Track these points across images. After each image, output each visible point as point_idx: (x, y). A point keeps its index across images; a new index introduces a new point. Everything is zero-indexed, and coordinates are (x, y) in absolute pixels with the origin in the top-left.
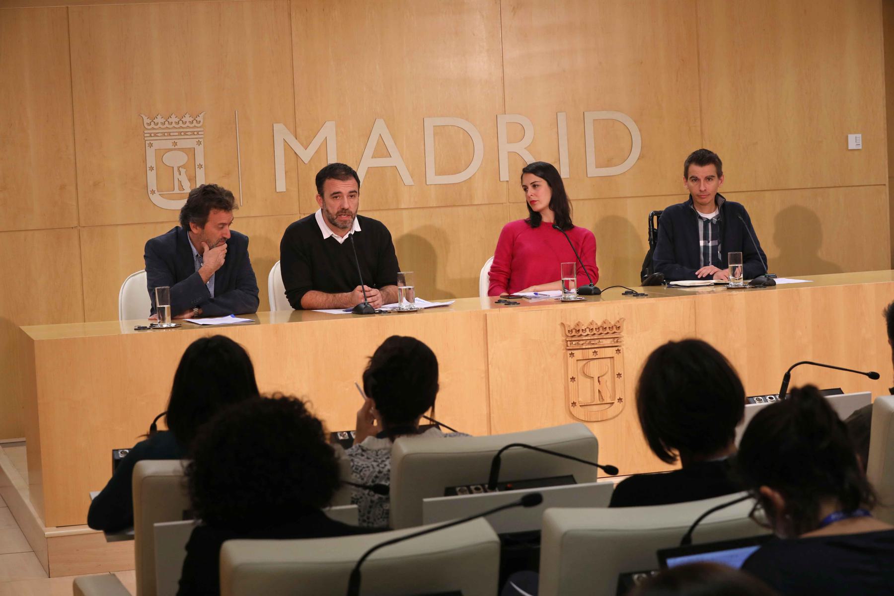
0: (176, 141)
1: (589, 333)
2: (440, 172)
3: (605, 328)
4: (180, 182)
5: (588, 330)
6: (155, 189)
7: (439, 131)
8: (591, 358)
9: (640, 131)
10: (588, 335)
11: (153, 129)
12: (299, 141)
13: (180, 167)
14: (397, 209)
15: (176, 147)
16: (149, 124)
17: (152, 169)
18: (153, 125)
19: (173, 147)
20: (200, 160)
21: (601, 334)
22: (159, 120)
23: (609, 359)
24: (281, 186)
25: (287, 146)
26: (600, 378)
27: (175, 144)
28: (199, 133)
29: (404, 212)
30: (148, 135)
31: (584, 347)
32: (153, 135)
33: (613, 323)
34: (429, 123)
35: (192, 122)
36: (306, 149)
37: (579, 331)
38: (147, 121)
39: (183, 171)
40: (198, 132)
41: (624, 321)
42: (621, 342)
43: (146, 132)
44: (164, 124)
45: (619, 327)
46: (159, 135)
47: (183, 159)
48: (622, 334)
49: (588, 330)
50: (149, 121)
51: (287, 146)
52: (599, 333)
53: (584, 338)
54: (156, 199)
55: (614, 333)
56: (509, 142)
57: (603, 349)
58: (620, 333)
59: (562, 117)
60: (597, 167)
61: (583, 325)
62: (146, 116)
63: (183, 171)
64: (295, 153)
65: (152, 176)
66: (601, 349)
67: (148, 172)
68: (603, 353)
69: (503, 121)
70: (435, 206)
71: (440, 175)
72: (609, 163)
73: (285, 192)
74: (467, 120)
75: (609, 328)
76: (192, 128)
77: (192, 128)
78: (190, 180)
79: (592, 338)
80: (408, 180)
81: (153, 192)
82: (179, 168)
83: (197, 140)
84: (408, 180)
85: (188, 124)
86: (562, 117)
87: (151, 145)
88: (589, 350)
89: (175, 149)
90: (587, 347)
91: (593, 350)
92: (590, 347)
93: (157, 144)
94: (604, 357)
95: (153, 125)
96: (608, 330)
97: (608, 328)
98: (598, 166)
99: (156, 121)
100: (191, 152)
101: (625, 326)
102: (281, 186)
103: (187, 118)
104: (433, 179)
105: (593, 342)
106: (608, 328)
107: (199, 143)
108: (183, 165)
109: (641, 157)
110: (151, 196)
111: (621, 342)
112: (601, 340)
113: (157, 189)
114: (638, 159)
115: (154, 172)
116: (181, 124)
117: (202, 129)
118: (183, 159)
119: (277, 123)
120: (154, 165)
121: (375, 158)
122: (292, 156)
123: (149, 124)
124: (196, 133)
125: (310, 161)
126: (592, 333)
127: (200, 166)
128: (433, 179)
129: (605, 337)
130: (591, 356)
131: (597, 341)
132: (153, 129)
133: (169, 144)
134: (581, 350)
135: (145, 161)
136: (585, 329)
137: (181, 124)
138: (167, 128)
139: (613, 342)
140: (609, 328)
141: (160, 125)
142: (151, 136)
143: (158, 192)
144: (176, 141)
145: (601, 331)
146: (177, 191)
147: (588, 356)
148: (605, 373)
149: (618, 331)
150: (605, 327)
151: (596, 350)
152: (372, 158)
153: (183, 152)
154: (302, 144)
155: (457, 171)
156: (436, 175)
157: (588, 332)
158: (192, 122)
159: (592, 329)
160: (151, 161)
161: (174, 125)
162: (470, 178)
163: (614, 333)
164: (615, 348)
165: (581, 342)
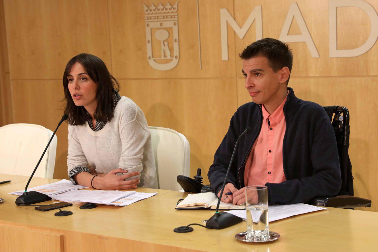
0: (162, 22)
4: (164, 51)
6: (151, 56)
11: (149, 14)
12: (237, 23)
13: (165, 41)
14: (307, 77)
15: (163, 27)
16: (147, 11)
17: (149, 42)
18: (149, 11)
19: (160, 27)
20: (176, 36)
22: (153, 8)
27: (161, 24)
28: (176, 17)
29: (312, 80)
30: (146, 18)
32: (149, 18)
35: (170, 9)
36: (241, 28)
38: (146, 8)
39: (166, 43)
40: (174, 16)
43: (146, 16)
44: (154, 10)
46: (153, 18)
47: (165, 35)
50: (147, 8)
54: (151, 62)
62: (145, 5)
63: (166, 43)
64: (235, 32)
65: (149, 46)
67: (148, 44)
70: (336, 75)
71: (342, 48)
73: (227, 61)
76: (172, 12)
77: (172, 12)
78: (170, 50)
80: (314, 53)
81: (150, 58)
82: (164, 41)
83: (174, 22)
84: (314, 53)
85: (168, 10)
87: (148, 25)
89: (163, 28)
93: (152, 25)
95: (149, 11)
99: (151, 8)
100: (169, 30)
102: (225, 57)
103: (168, 6)
107: (175, 24)
108: (167, 39)
110: (149, 60)
113: (152, 55)
115: (150, 44)
116: (165, 11)
117: (176, 14)
118: (165, 35)
119: (222, 7)
120: (150, 40)
121: (290, 35)
122: (231, 33)
123: (147, 11)
124: (173, 17)
127: (175, 41)
128: (334, 53)
132: (149, 14)
133: (158, 25)
135: (145, 37)
137: (165, 11)
138: (157, 13)
141: (153, 11)
142: (148, 19)
143: (153, 57)
144: (162, 22)
146: (163, 58)
152: (288, 35)
153: (167, 30)
155: (355, 47)
156: (337, 49)
158: (170, 9)
160: (148, 37)
161: (161, 11)
162: (367, 52)
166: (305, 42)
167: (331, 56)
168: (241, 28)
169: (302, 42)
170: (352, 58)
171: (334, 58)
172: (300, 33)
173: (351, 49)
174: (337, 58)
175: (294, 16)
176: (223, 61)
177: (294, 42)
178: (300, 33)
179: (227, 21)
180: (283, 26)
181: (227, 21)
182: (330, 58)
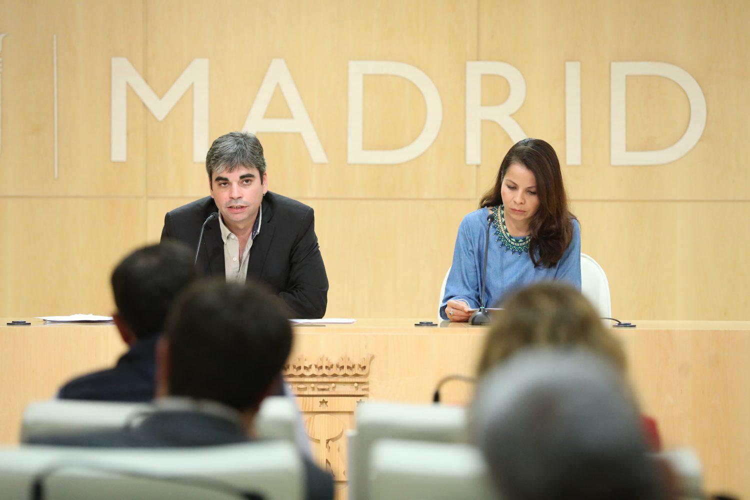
1: (316, 373)
2: (368, 146)
3: (343, 367)
5: (313, 367)
7: (372, 82)
8: (317, 410)
9: (705, 95)
10: (313, 376)
21: (335, 375)
23: (347, 416)
24: (119, 152)
25: (131, 93)
26: (330, 442)
31: (306, 393)
33: (356, 361)
34: (357, 70)
36: (160, 97)
37: (300, 368)
41: (373, 357)
42: (367, 390)
45: (364, 367)
48: (370, 378)
49: (313, 367)
51: (131, 93)
52: (332, 374)
53: (306, 380)
55: (356, 375)
56: (485, 103)
57: (337, 398)
58: (366, 376)
59: (573, 70)
60: (628, 149)
61: (306, 360)
64: (144, 106)
66: (334, 398)
68: (335, 404)
69: (475, 70)
72: (649, 145)
73: (123, 162)
74: (418, 67)
75: (348, 367)
79: (320, 380)
80: (318, 154)
84: (318, 154)
86: (573, 70)
88: (314, 398)
90: (312, 393)
91: (321, 399)
92: (315, 393)
94: (337, 410)
96: (346, 371)
97: (345, 368)
98: (628, 149)
101: (374, 368)
102: (119, 152)
104: (357, 154)
105: (321, 387)
106: (345, 368)
109: (704, 137)
111: (367, 390)
112: (333, 385)
114: (700, 140)
125: (166, 118)
126: (320, 373)
129: (341, 380)
130: (317, 408)
131: (326, 387)
134: (302, 398)
136: (310, 366)
139: (354, 389)
140: (348, 367)
145: (334, 371)
147: (313, 408)
148: (337, 435)
149: (361, 374)
150: (341, 365)
151: (326, 399)
154: (155, 91)
155: (398, 146)
157: (314, 371)
159: (321, 367)
162: (418, 157)
163: (356, 375)
164: (355, 398)
165: (302, 386)
166: (299, 134)
167: (351, 159)
168: (160, 97)
169: (294, 134)
170: (391, 165)
171: (355, 165)
172: (290, 116)
173: (390, 149)
174: (362, 165)
175: (278, 85)
176: (114, 162)
177: (278, 133)
178: (290, 116)
179: (128, 84)
180: (253, 99)
181: (128, 84)
182: (350, 165)
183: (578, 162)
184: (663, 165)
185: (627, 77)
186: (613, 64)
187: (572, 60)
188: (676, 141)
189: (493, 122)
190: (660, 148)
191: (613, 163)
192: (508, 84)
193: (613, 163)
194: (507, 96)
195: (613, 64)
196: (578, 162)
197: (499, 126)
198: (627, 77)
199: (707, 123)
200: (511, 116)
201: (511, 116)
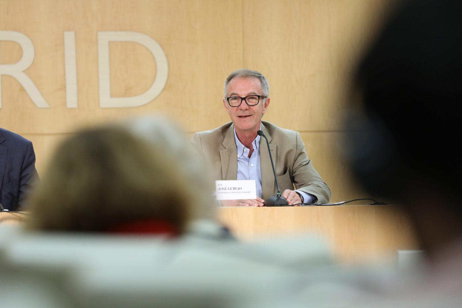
9: (167, 56)
59: (69, 38)
60: (112, 96)
72: (127, 92)
86: (69, 38)
98: (112, 96)
114: (164, 89)
183: (75, 106)
184: (138, 107)
185: (110, 42)
186: (100, 34)
187: (68, 30)
188: (147, 90)
189: (10, 77)
190: (135, 95)
191: (102, 106)
192: (20, 48)
193: (102, 106)
194: (20, 56)
195: (100, 34)
196: (75, 106)
197: (15, 79)
198: (110, 42)
199: (169, 77)
200: (24, 71)
201: (24, 71)
